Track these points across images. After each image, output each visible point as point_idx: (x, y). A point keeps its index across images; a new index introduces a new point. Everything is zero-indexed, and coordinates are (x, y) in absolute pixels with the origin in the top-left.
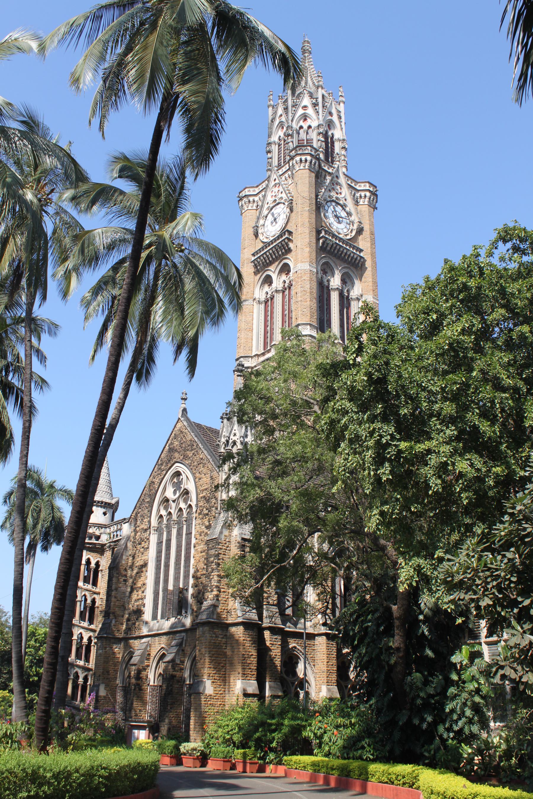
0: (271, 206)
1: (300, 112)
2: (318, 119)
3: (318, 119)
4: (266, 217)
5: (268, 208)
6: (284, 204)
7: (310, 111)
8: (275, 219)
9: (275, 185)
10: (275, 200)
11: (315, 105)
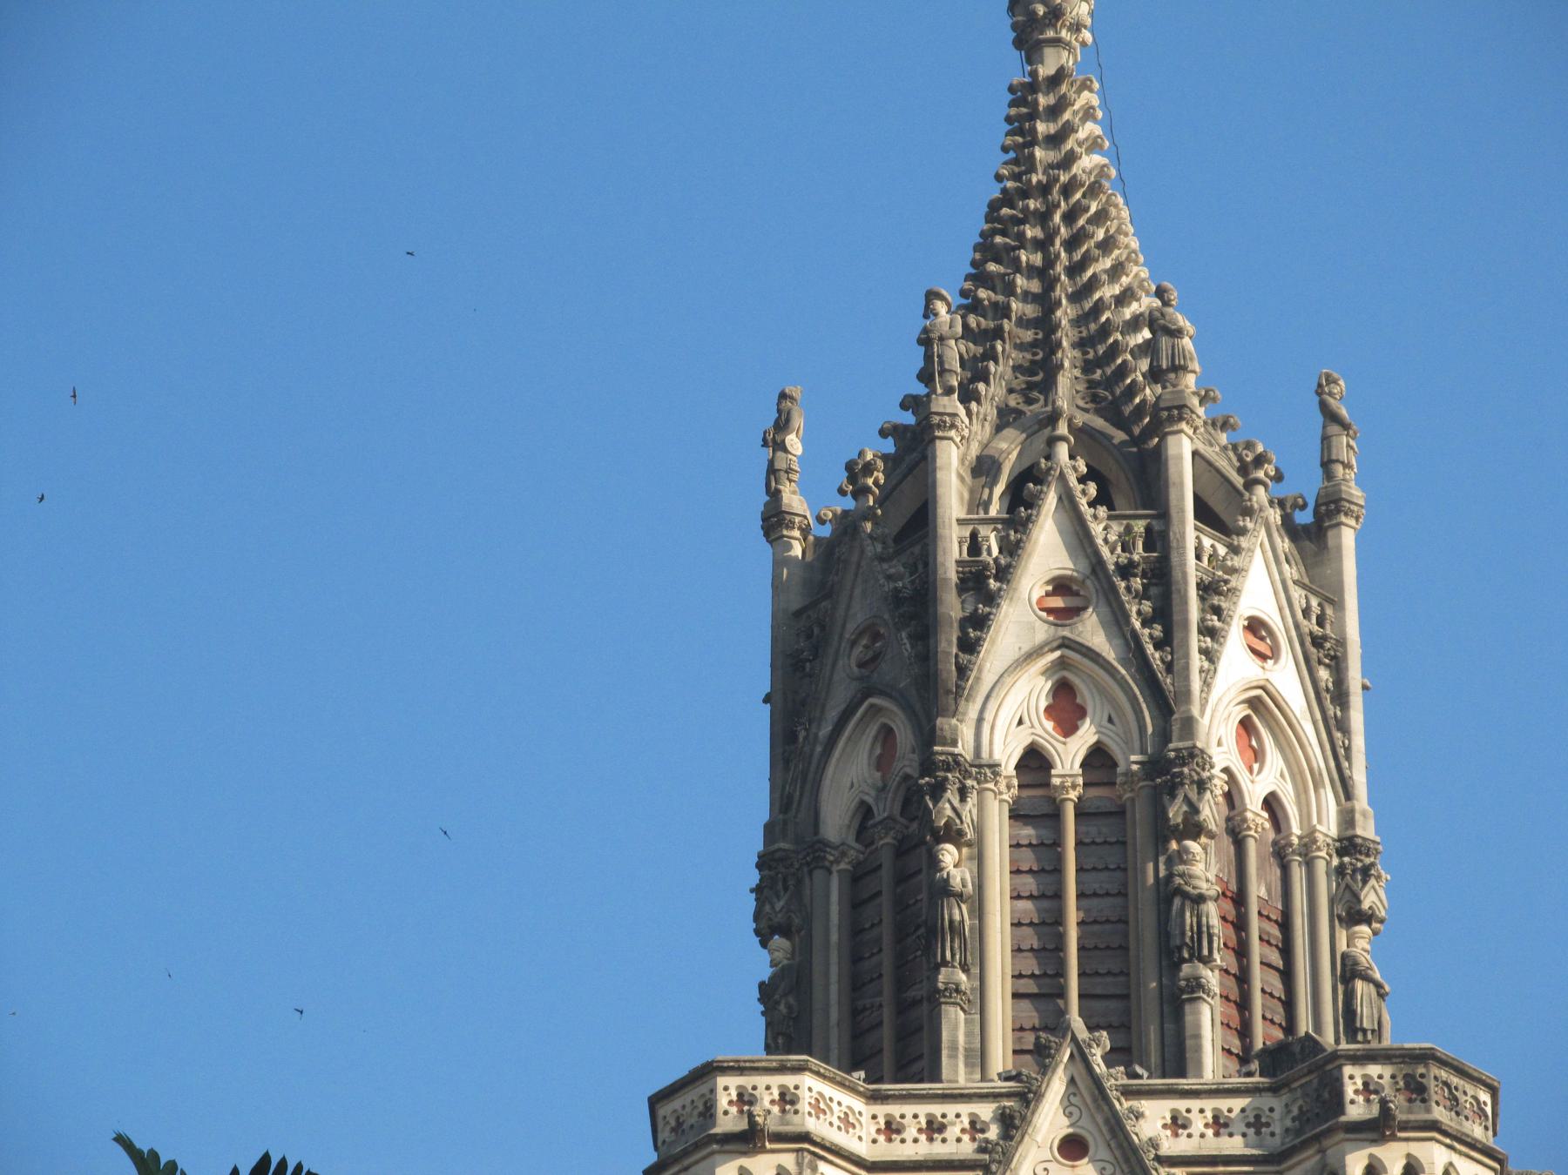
2: (1345, 787)
3: (1345, 787)
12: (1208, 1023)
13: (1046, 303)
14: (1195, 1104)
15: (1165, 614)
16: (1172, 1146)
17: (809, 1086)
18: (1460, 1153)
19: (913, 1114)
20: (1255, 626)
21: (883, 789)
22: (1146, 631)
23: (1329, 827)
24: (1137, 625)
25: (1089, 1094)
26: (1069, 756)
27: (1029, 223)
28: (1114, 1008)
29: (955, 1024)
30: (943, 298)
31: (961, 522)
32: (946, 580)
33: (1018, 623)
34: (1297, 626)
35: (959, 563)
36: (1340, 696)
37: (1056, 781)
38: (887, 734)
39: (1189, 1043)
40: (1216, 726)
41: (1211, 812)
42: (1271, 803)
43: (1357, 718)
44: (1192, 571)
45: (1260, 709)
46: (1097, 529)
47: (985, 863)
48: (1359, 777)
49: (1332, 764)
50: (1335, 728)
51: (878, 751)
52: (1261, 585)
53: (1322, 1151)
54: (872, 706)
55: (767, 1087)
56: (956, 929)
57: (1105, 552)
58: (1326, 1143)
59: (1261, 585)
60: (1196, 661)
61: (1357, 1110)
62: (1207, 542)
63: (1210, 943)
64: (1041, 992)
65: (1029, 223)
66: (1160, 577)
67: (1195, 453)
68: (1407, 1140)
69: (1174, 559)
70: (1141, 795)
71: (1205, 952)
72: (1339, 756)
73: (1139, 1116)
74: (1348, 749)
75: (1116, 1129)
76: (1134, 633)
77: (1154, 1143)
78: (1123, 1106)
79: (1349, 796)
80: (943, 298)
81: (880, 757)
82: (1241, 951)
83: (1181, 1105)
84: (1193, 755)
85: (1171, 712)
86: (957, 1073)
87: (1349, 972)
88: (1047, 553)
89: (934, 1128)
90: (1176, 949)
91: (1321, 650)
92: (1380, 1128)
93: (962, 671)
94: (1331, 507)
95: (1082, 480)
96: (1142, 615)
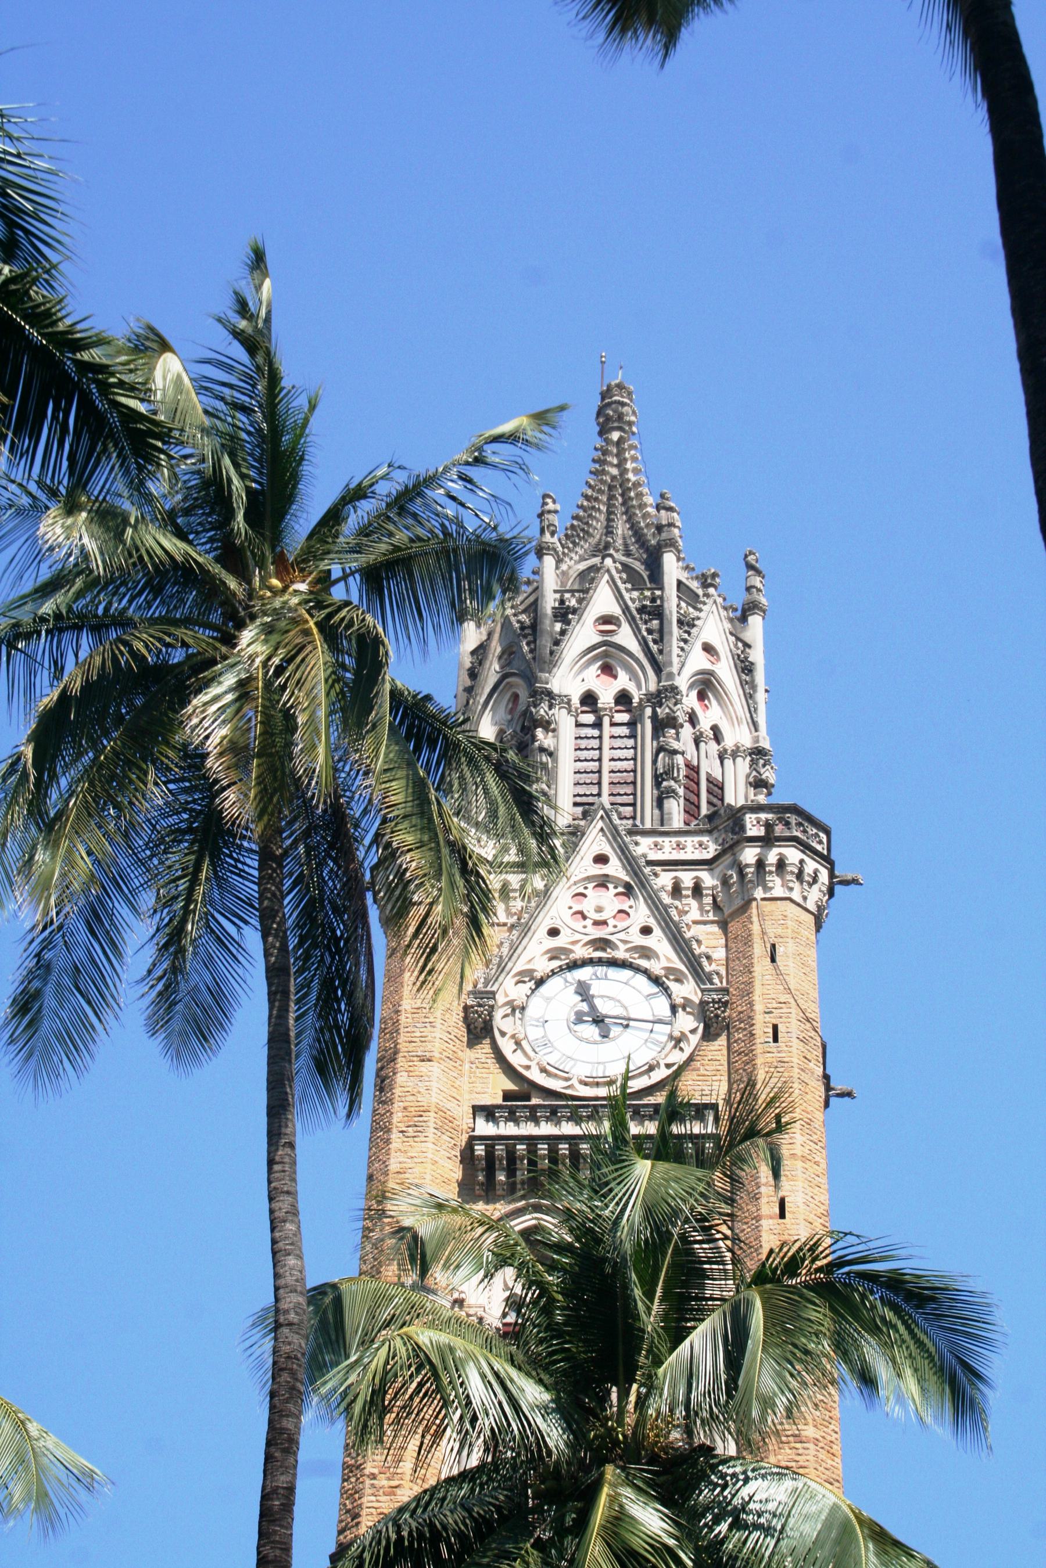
0: (581, 952)
1: (698, 661)
4: (540, 982)
6: (656, 980)
7: (726, 672)
8: (599, 1021)
9: (603, 882)
10: (602, 944)
11: (745, 668)
14: (667, 839)
18: (808, 856)
20: (708, 648)
21: (510, 721)
22: (650, 637)
24: (645, 634)
30: (550, 497)
31: (555, 591)
32: (546, 615)
33: (584, 634)
34: (731, 651)
35: (553, 608)
37: (599, 705)
38: (516, 697)
39: (665, 816)
43: (761, 696)
46: (627, 596)
48: (762, 719)
49: (748, 715)
50: (749, 697)
51: (510, 706)
52: (713, 626)
53: (734, 854)
54: (508, 683)
56: (544, 766)
57: (630, 603)
58: (736, 850)
59: (713, 626)
60: (676, 651)
62: (683, 604)
63: (678, 772)
66: (655, 611)
67: (680, 583)
68: (779, 846)
71: (675, 775)
72: (752, 711)
73: (637, 844)
74: (756, 710)
76: (643, 638)
77: (644, 856)
78: (627, 839)
79: (756, 730)
80: (550, 497)
81: (512, 709)
83: (660, 840)
85: (661, 671)
93: (552, 653)
95: (618, 571)
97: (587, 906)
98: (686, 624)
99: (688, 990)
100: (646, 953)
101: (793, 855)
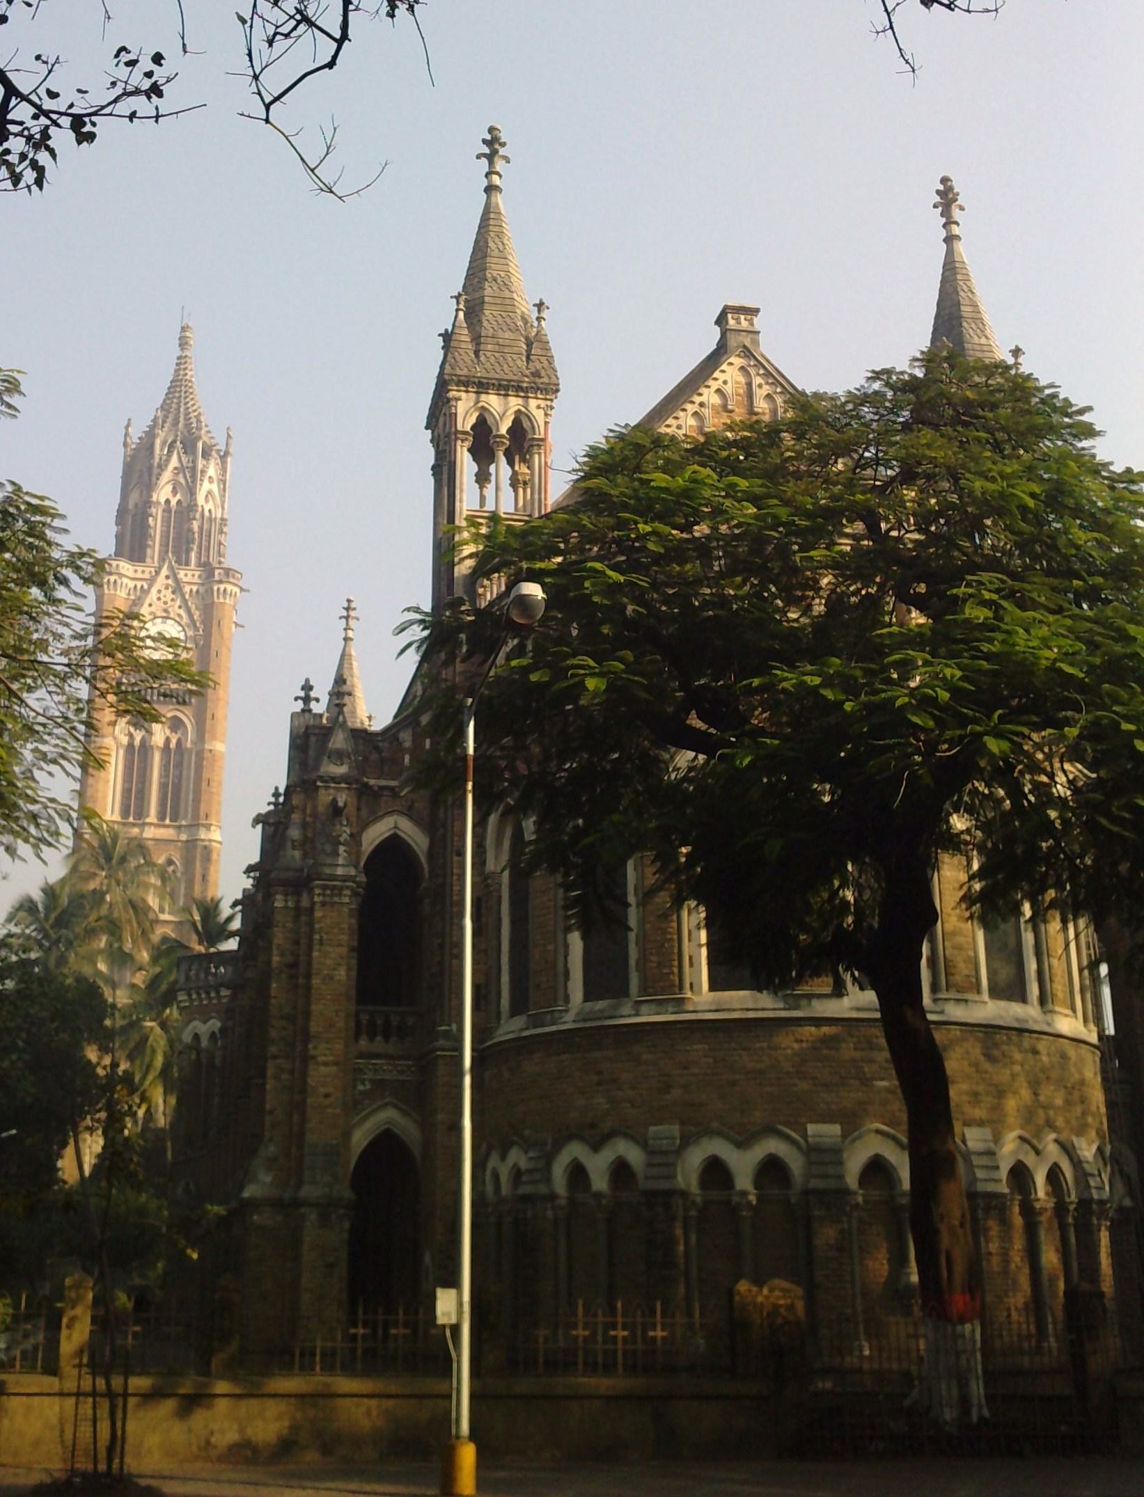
0: (159, 613)
2: (223, 508)
3: (223, 508)
5: (151, 613)
7: (215, 488)
12: (193, 555)
13: (179, 404)
15: (194, 476)
16: (185, 580)
17: (121, 564)
19: (140, 569)
23: (219, 516)
25: (171, 568)
26: (174, 502)
27: (178, 388)
28: (177, 553)
29: (149, 551)
33: (167, 475)
36: (224, 490)
40: (201, 500)
41: (198, 516)
42: (210, 511)
44: (200, 466)
45: (210, 492)
47: (156, 523)
55: (114, 563)
59: (212, 471)
61: (217, 578)
64: (165, 545)
65: (178, 388)
66: (194, 469)
69: (146, 792)
70: (187, 510)
72: (223, 502)
75: (175, 575)
82: (201, 543)
84: (196, 505)
86: (148, 560)
87: (220, 543)
88: (174, 462)
89: (143, 572)
90: (190, 541)
91: (223, 481)
92: (220, 582)
94: (227, 453)
96: (189, 480)
97: (162, 595)
98: (203, 472)
99: (190, 633)
100: (179, 615)
101: (229, 587)
